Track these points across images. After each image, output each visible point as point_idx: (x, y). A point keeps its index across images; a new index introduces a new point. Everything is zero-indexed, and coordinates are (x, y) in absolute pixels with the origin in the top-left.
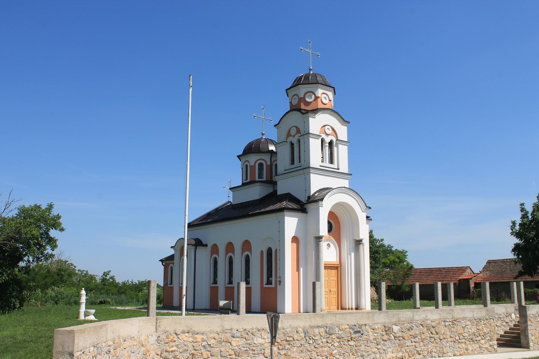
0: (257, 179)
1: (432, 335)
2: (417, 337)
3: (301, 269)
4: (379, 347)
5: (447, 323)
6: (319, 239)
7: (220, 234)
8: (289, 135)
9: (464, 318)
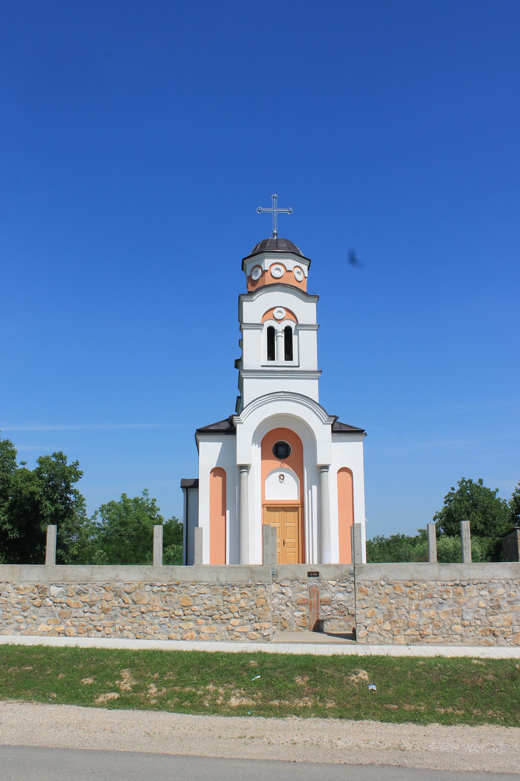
1: (123, 605)
2: (94, 605)
3: (228, 512)
4: (25, 614)
5: (156, 589)
9: (195, 583)
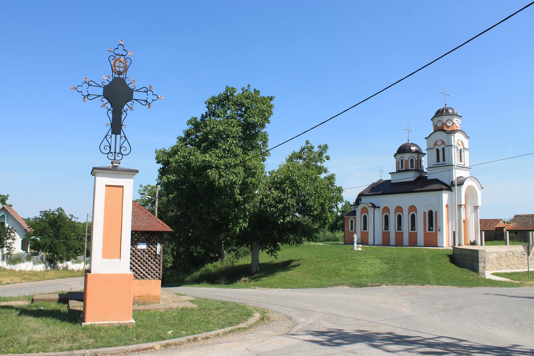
0: (410, 169)
6: (460, 206)
7: (391, 201)
8: (436, 144)
